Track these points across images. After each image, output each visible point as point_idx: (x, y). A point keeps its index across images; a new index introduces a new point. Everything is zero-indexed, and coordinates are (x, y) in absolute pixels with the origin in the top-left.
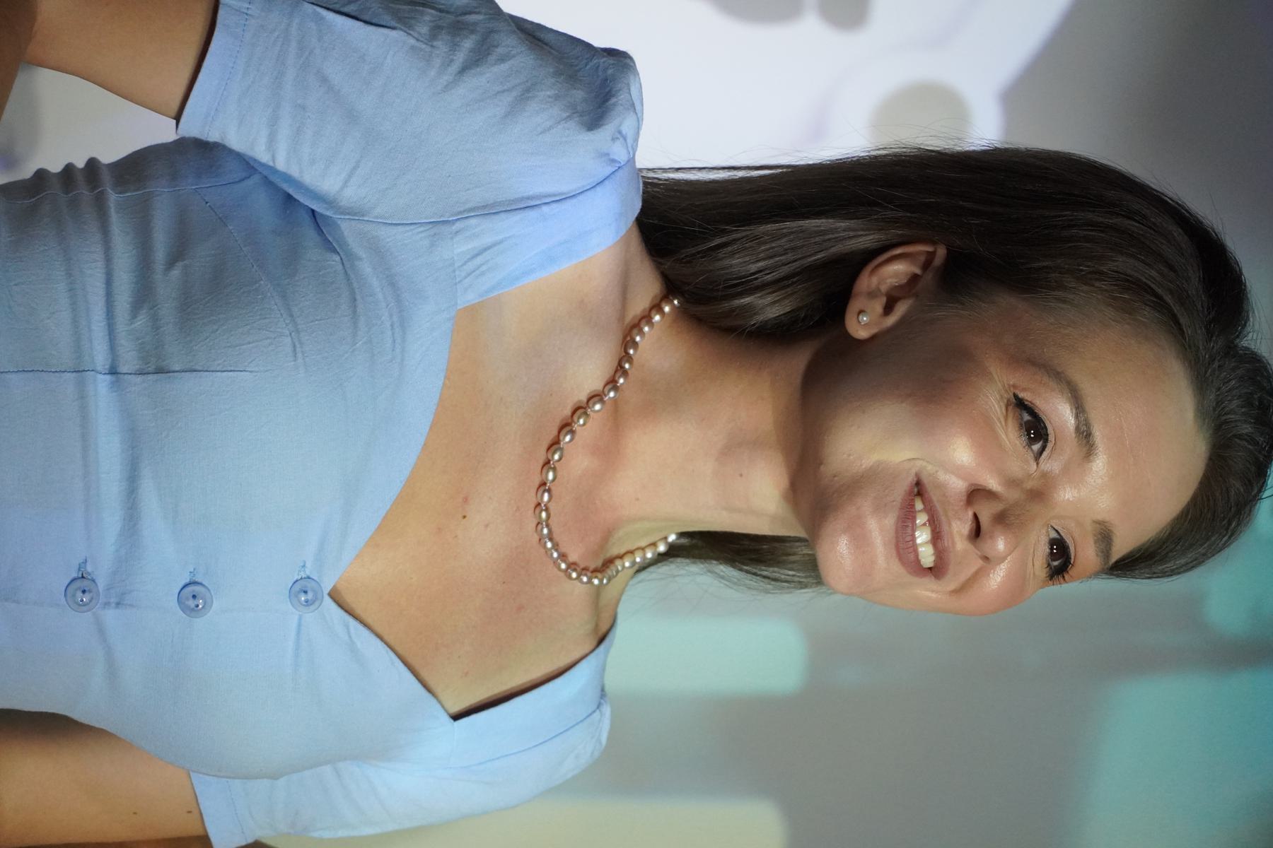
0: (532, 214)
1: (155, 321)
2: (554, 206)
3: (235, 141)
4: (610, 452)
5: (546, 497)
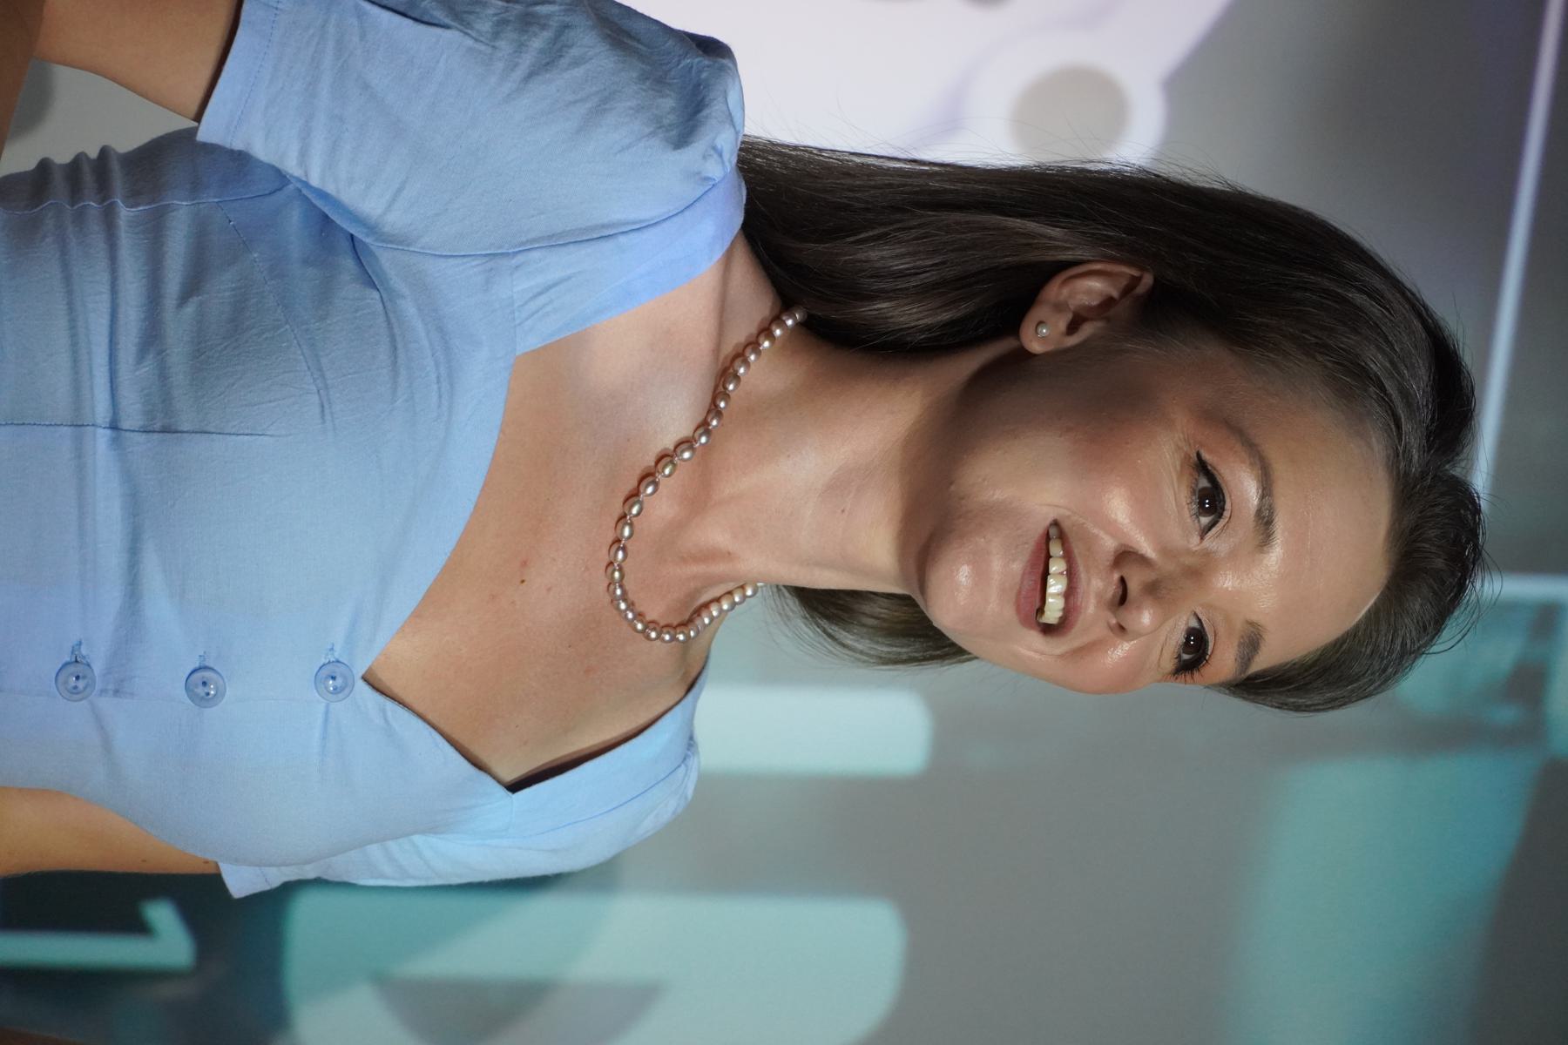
0: (607, 246)
1: (163, 374)
2: (631, 236)
3: (261, 150)
4: (699, 501)
5: (620, 555)
